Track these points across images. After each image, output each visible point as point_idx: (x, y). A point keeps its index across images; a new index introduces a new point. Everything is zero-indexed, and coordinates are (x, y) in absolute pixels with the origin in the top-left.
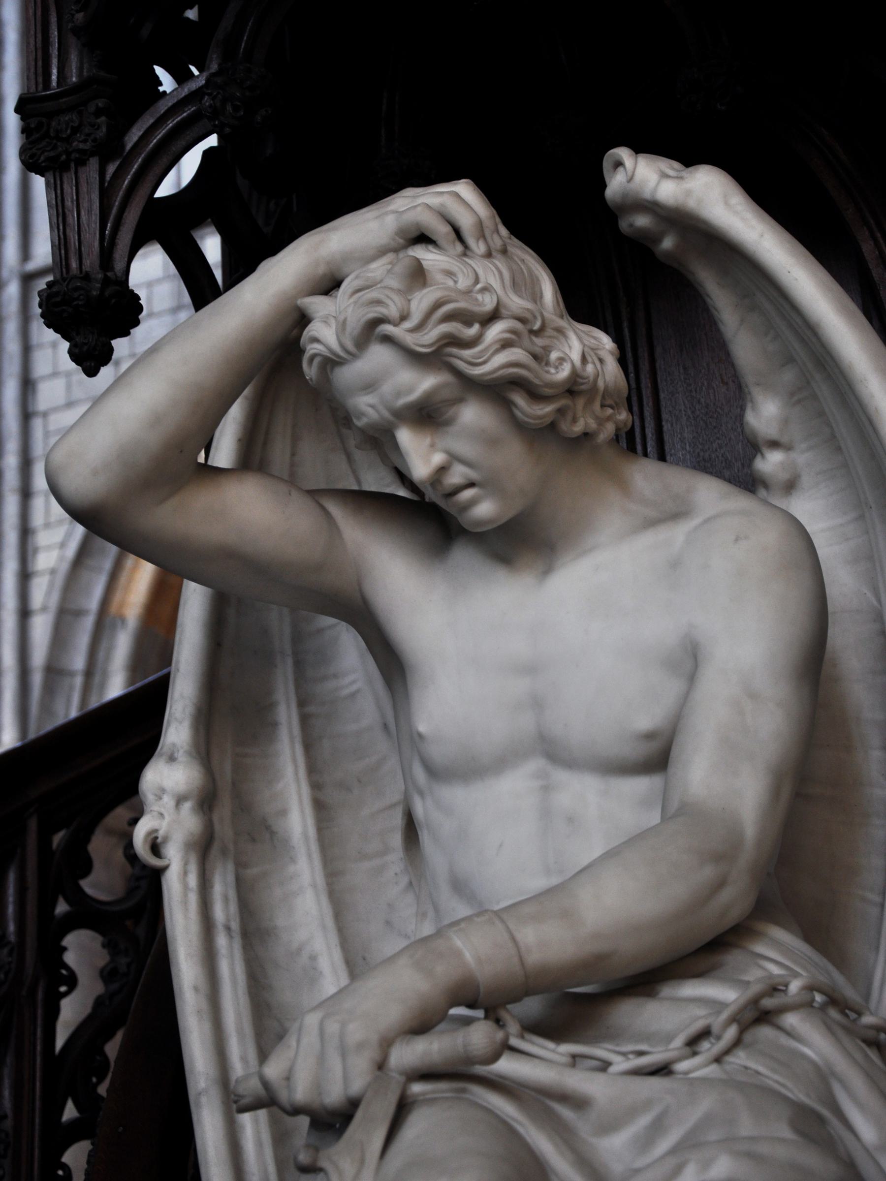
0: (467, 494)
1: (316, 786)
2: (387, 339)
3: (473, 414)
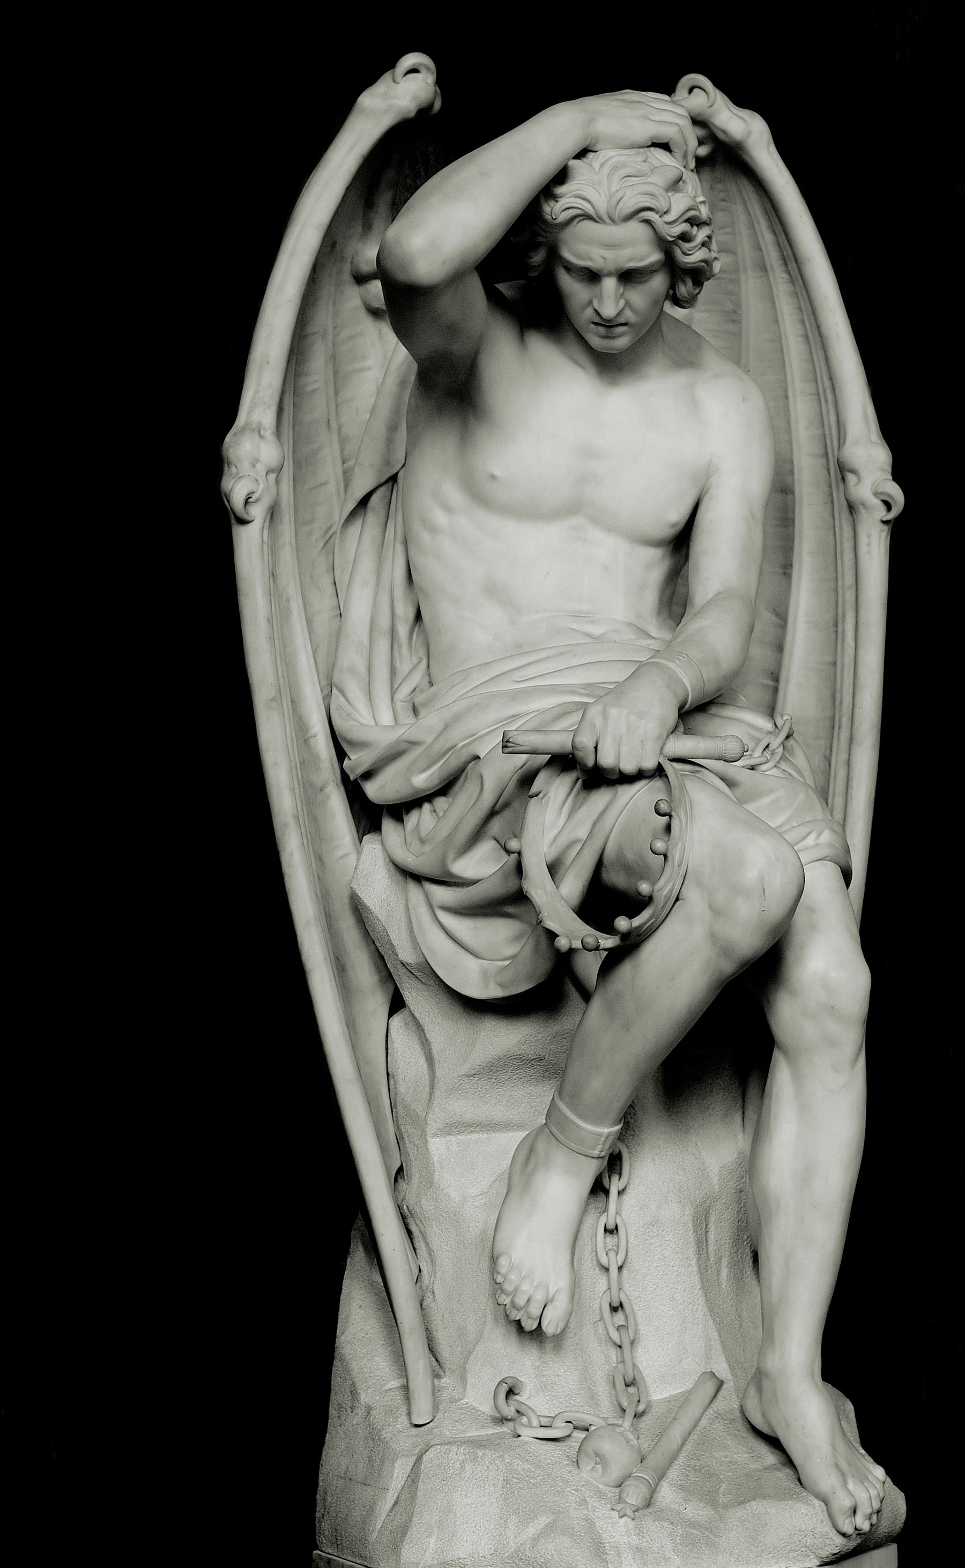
2: (647, 222)
3: (658, 282)
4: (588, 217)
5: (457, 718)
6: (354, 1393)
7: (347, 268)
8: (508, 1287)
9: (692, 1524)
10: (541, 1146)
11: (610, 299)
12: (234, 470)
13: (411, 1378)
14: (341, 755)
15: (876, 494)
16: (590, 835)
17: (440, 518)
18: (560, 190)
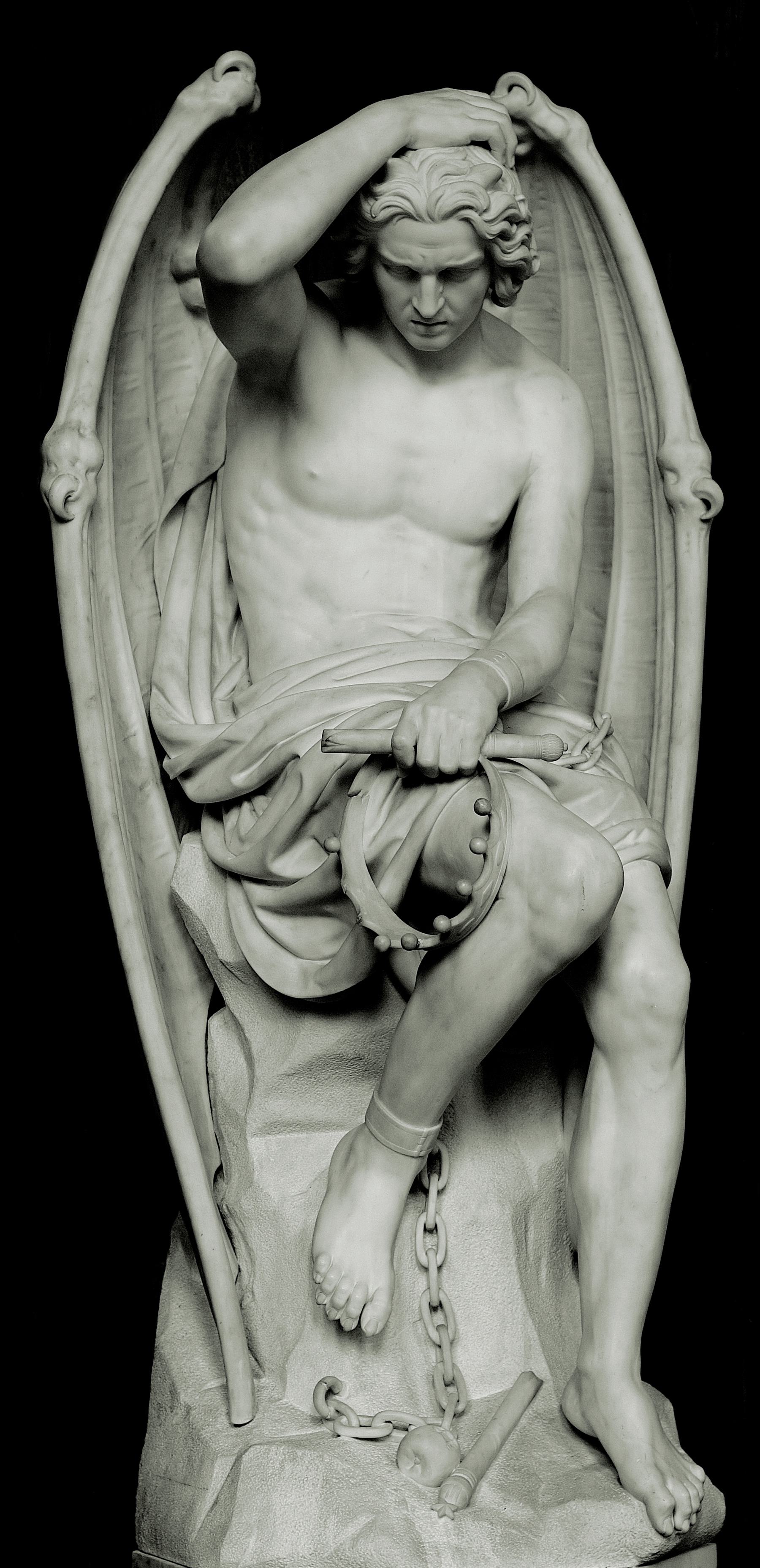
2: (467, 220)
3: (478, 281)
4: (407, 215)
5: (276, 717)
6: (174, 1393)
7: (166, 266)
8: (328, 1287)
9: (512, 1524)
10: (360, 1146)
11: (429, 297)
12: (53, 469)
13: (230, 1377)
14: (161, 754)
15: (695, 493)
16: (410, 834)
17: (260, 516)
18: (379, 188)
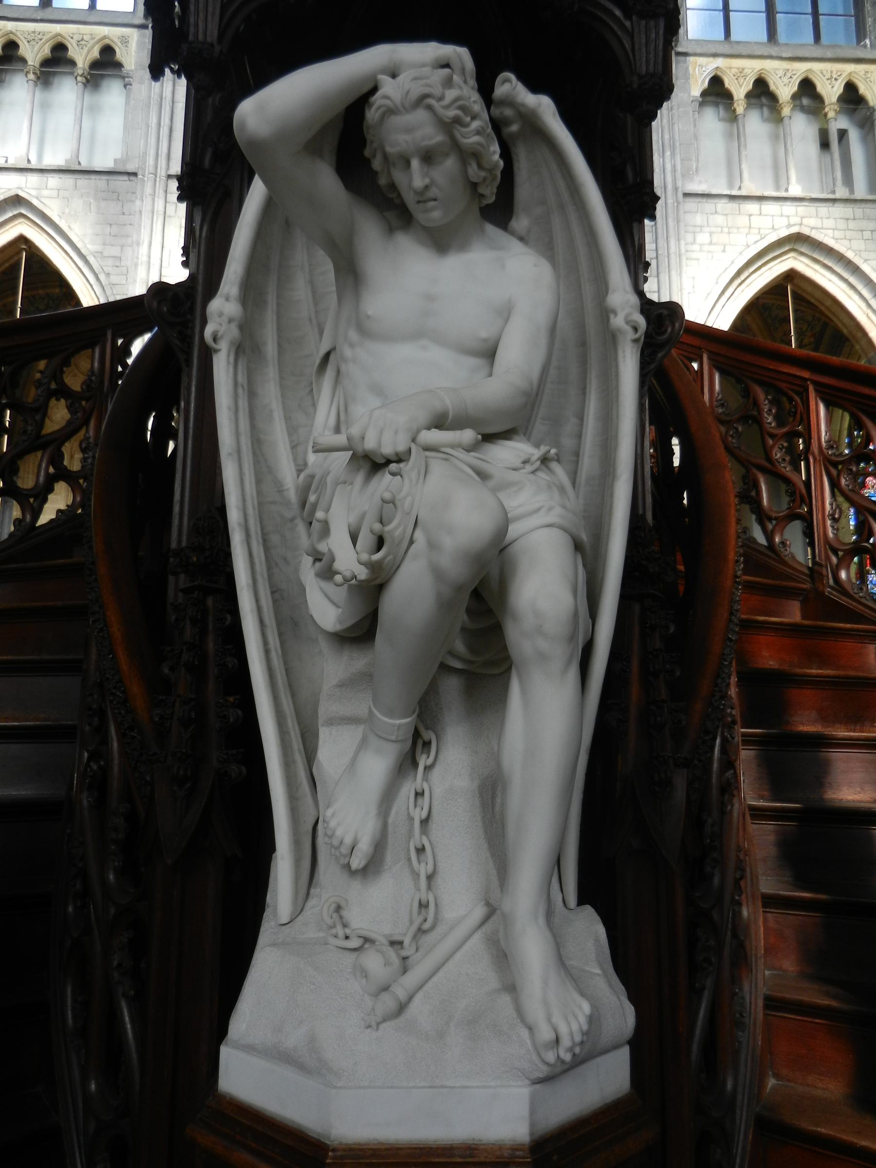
0: (432, 203)
1: (279, 337)
2: (429, 108)
3: (450, 163)
17: (348, 352)
